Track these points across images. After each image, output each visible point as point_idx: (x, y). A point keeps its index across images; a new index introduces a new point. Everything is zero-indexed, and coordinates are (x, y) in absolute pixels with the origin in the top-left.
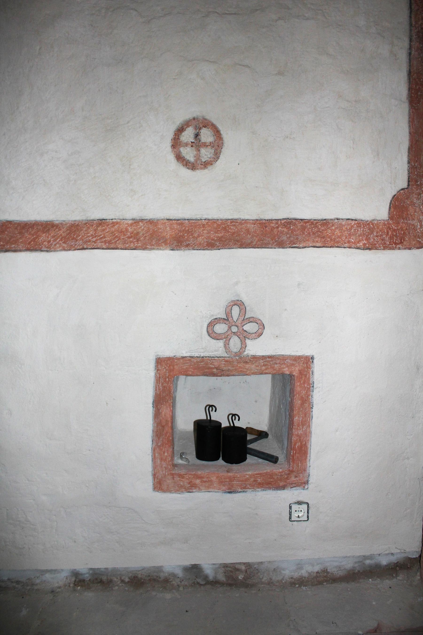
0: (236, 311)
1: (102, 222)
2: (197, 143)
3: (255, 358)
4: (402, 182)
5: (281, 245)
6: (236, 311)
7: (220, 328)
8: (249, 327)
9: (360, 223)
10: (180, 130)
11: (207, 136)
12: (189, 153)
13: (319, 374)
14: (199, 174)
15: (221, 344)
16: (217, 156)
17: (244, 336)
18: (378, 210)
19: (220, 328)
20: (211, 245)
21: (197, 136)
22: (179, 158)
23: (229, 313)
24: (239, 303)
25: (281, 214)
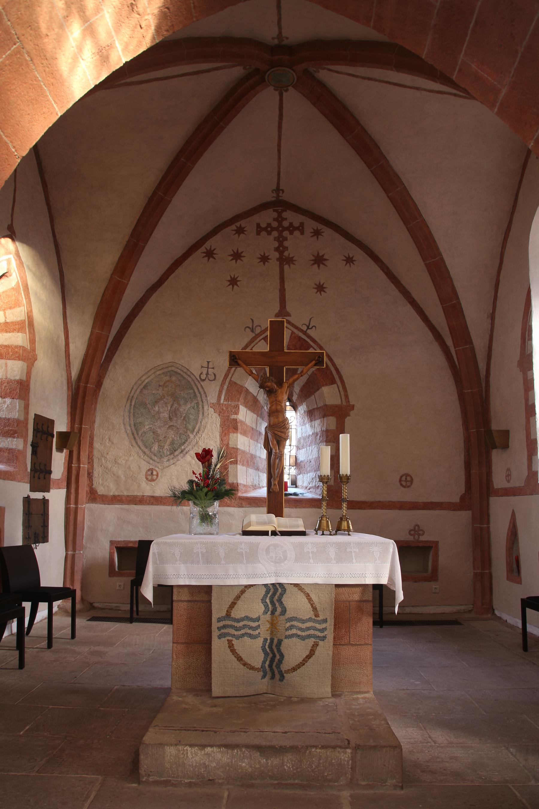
0: (417, 528)
1: (380, 502)
2: (406, 481)
3: (422, 541)
4: (463, 492)
5: (429, 509)
6: (417, 528)
7: (412, 532)
8: (421, 532)
9: (451, 503)
10: (401, 477)
11: (409, 479)
12: (404, 483)
13: (440, 545)
14: (407, 489)
15: (412, 537)
16: (411, 484)
17: (419, 535)
18: (456, 499)
19: (412, 532)
20: (410, 509)
21: (406, 479)
22: (401, 485)
23: (415, 528)
24: (418, 526)
25: (429, 501)
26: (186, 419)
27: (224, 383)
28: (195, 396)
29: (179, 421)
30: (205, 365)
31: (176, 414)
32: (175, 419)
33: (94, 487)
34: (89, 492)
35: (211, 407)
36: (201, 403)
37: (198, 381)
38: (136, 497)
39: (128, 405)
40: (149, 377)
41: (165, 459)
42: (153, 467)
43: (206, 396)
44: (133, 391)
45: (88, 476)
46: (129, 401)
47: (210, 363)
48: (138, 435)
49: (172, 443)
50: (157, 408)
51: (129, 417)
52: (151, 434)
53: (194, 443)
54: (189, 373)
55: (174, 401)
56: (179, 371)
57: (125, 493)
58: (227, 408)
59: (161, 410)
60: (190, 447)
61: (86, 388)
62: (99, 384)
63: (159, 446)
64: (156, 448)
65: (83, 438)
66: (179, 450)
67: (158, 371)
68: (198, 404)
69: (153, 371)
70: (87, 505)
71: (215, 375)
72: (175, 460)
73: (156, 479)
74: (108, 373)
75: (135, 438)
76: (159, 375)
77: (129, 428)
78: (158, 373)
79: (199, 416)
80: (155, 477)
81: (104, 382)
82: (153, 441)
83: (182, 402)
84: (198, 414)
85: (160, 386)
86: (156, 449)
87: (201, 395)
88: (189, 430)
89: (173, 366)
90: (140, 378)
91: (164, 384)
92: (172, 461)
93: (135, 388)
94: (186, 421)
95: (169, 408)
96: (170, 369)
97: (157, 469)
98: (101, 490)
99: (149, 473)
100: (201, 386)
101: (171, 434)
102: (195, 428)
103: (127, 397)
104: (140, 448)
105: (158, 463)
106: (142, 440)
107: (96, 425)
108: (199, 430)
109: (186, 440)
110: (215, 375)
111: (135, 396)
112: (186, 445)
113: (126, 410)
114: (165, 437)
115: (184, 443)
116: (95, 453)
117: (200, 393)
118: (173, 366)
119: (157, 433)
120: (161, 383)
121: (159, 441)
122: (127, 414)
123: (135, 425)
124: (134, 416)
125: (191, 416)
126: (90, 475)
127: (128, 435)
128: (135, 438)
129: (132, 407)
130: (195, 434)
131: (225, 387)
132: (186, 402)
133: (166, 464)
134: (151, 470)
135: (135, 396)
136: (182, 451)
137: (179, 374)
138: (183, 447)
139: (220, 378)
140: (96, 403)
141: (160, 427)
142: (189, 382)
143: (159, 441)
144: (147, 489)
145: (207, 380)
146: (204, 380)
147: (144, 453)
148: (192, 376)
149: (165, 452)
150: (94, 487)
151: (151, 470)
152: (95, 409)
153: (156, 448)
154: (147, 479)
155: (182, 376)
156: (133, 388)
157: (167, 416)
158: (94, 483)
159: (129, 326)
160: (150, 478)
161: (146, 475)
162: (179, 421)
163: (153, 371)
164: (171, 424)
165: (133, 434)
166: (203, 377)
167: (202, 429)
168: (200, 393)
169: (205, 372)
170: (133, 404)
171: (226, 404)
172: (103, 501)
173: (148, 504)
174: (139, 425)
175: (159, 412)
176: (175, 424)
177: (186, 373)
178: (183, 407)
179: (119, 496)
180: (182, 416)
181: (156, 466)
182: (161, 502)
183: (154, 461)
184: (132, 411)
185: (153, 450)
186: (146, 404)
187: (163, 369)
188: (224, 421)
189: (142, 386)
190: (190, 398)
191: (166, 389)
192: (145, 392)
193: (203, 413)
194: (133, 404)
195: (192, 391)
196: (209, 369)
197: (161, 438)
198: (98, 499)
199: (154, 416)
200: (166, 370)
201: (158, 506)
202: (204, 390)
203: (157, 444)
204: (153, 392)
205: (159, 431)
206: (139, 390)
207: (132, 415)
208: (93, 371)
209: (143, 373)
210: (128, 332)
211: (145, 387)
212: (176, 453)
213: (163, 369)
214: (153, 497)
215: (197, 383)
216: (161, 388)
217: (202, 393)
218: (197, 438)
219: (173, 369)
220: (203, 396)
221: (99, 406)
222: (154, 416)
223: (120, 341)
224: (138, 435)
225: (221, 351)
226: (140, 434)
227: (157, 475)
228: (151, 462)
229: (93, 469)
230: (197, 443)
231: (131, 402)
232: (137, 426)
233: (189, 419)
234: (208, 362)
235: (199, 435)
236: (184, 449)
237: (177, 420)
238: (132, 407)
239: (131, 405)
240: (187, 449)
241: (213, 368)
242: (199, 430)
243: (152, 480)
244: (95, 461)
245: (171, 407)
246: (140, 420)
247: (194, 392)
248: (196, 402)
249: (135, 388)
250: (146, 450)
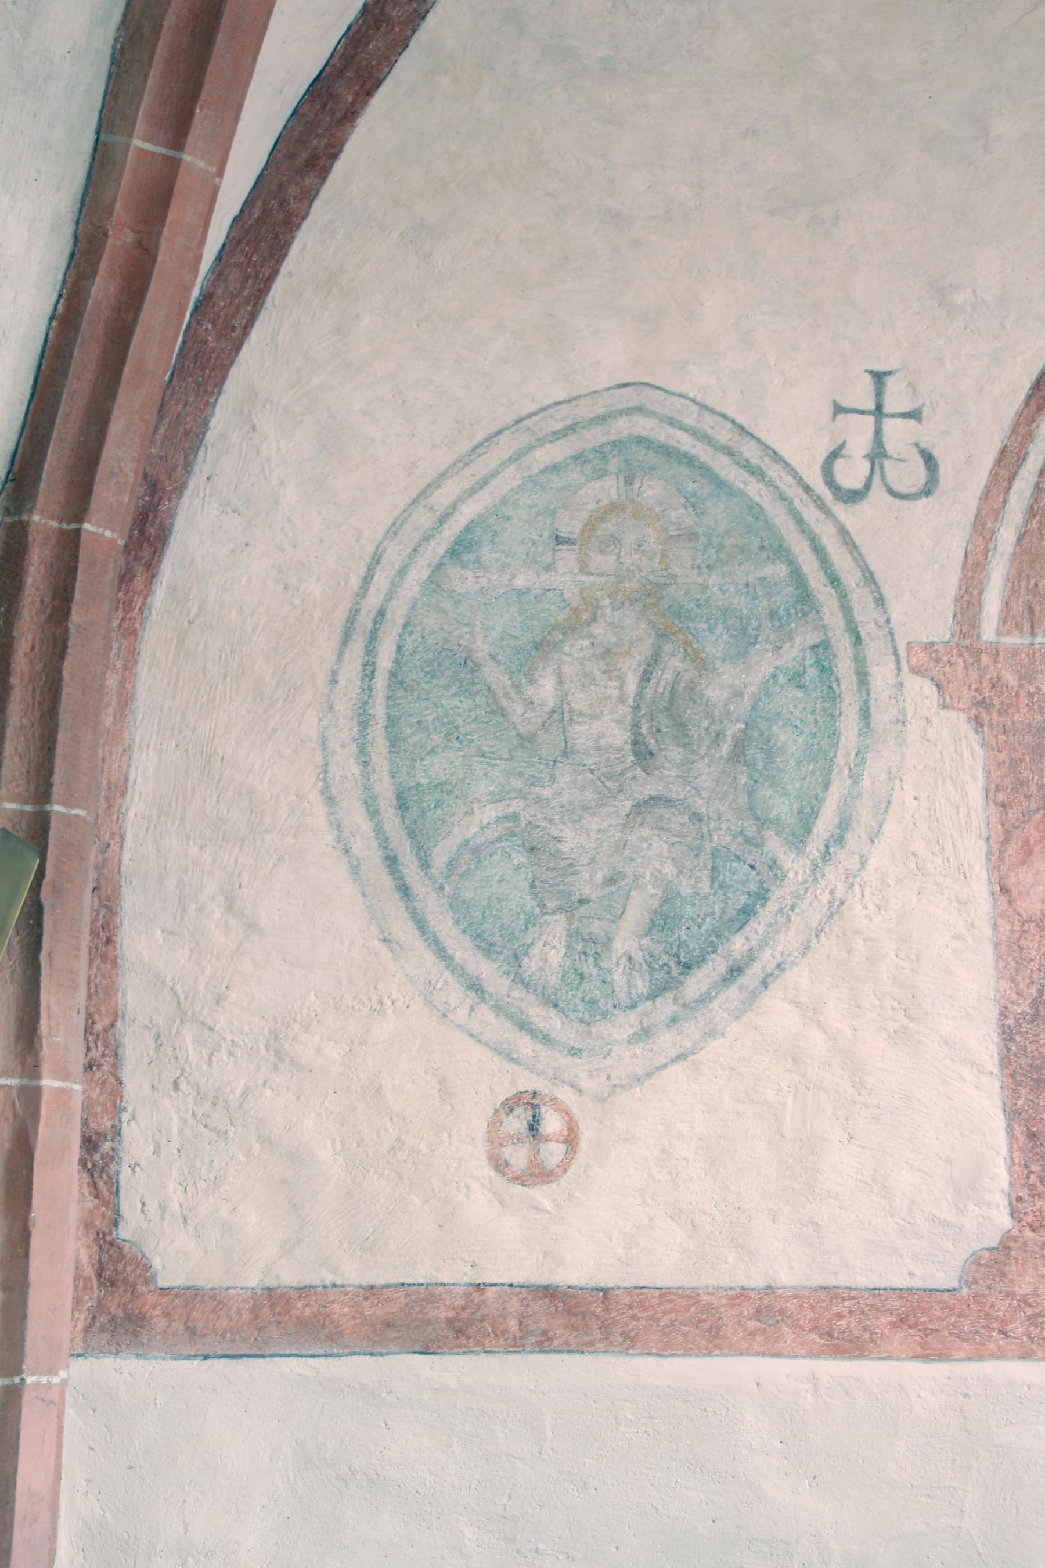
26: (749, 749)
27: (997, 514)
28: (805, 597)
29: (706, 772)
30: (862, 395)
31: (680, 726)
32: (676, 753)
33: (124, 1232)
34: (89, 1272)
35: (915, 671)
36: (843, 646)
37: (819, 503)
38: (427, 1294)
39: (351, 669)
40: (484, 483)
41: (621, 1027)
42: (540, 1085)
43: (880, 601)
44: (381, 581)
45: (83, 1162)
46: (358, 645)
47: (891, 385)
48: (425, 865)
49: (663, 918)
50: (546, 690)
51: (362, 751)
52: (520, 858)
53: (813, 912)
54: (750, 451)
55: (663, 636)
56: (684, 442)
57: (354, 1273)
58: (1026, 676)
59: (579, 700)
60: (789, 940)
61: (70, 545)
62: (148, 536)
63: (573, 935)
64: (550, 952)
65: (56, 891)
66: (717, 965)
67: (541, 442)
68: (823, 648)
69: (507, 446)
70: (79, 1371)
71: (929, 460)
72: (692, 1030)
73: (564, 1167)
74: (204, 463)
75: (405, 891)
76: (554, 468)
77: (365, 825)
78: (545, 456)
79: (834, 736)
80: (553, 1153)
81: (180, 523)
82: (529, 902)
83: (715, 643)
84: (832, 717)
85: (559, 540)
86: (555, 957)
87: (843, 595)
88: (777, 822)
89: (639, 409)
90: (424, 493)
91: (590, 526)
92: (666, 1041)
93: (394, 556)
94: (751, 765)
95: (632, 685)
96: (623, 427)
97: (565, 1094)
98: (176, 1256)
99: (516, 1123)
100: (843, 532)
101: (655, 857)
102: (815, 814)
103: (341, 615)
104: (442, 954)
105: (574, 1052)
106: (456, 904)
107: (136, 807)
108: (844, 825)
109: (762, 896)
110: (929, 460)
111: (397, 613)
112: (757, 927)
113: (343, 706)
114: (611, 881)
115: (747, 913)
116: (135, 996)
117: (834, 581)
118: (639, 409)
119: (557, 855)
120: (570, 525)
121: (573, 905)
122: (345, 730)
123: (402, 803)
124: (394, 741)
125: (783, 736)
126: (98, 1154)
127: (355, 869)
128: (405, 891)
129: (380, 683)
130: (814, 848)
131: (1007, 536)
132: (744, 640)
133: (630, 1059)
134: (530, 1105)
135: (397, 613)
136: (735, 971)
137: (689, 460)
138: (738, 944)
139: (967, 478)
140: (132, 657)
141: (575, 814)
142: (756, 510)
143: (573, 905)
144: (507, 1242)
145: (877, 491)
146: (854, 496)
147: (476, 987)
148: (774, 472)
149: (618, 977)
150: (124, 1232)
151: (530, 1105)
152: (126, 700)
153: (550, 952)
154: (500, 1166)
155: (705, 470)
156: (376, 559)
157: (619, 737)
158: (128, 1205)
159: (333, 153)
160: (518, 1157)
161: (495, 1141)
162: (706, 772)
163: (507, 446)
164: (651, 789)
165: (392, 862)
166: (851, 473)
167: (864, 815)
168: (834, 581)
169: (859, 436)
170: (385, 660)
171: (1014, 652)
172: (192, 1332)
173: (517, 1345)
174: (430, 800)
175: (561, 715)
176: (677, 791)
177: (730, 453)
178: (728, 675)
179: (302, 1291)
180: (719, 736)
181: (556, 1078)
182: (606, 1328)
183: (546, 1039)
184: (379, 709)
185: (531, 965)
186: (470, 664)
187: (572, 428)
188: (1014, 765)
189: (439, 547)
190: (773, 614)
191: (602, 562)
192: (464, 581)
193: (865, 713)
194: (385, 660)
195: (781, 570)
196: (888, 424)
197: (586, 883)
198: (160, 1323)
199: (527, 740)
200: (596, 436)
201: (587, 1359)
202: (860, 561)
203: (558, 926)
204: (520, 582)
205: (570, 839)
206: (419, 573)
207: (377, 733)
208: (117, 426)
209: (444, 458)
210: (328, 189)
211: (461, 549)
212: (697, 983)
213: (572, 428)
214: (549, 1292)
215: (810, 513)
216: (568, 556)
217: (850, 575)
218: (833, 876)
219: (644, 426)
220: (860, 598)
221: (150, 683)
222: (532, 738)
223: (278, 251)
224: (425, 865)
225: (962, 298)
226: (440, 859)
227: (571, 1140)
228: (525, 1045)
229: (117, 1110)
230: (836, 908)
231: (370, 650)
232: (415, 810)
233: (770, 754)
234: (879, 378)
235: (845, 860)
236: (751, 956)
237: (686, 764)
238: (380, 683)
239: (369, 672)
240: (767, 959)
241: (914, 415)
242: (844, 825)
243: (539, 1174)
244: (134, 1047)
245: (646, 678)
246: (437, 767)
247: (797, 575)
248: (814, 638)
249: (394, 556)
250: (485, 969)
